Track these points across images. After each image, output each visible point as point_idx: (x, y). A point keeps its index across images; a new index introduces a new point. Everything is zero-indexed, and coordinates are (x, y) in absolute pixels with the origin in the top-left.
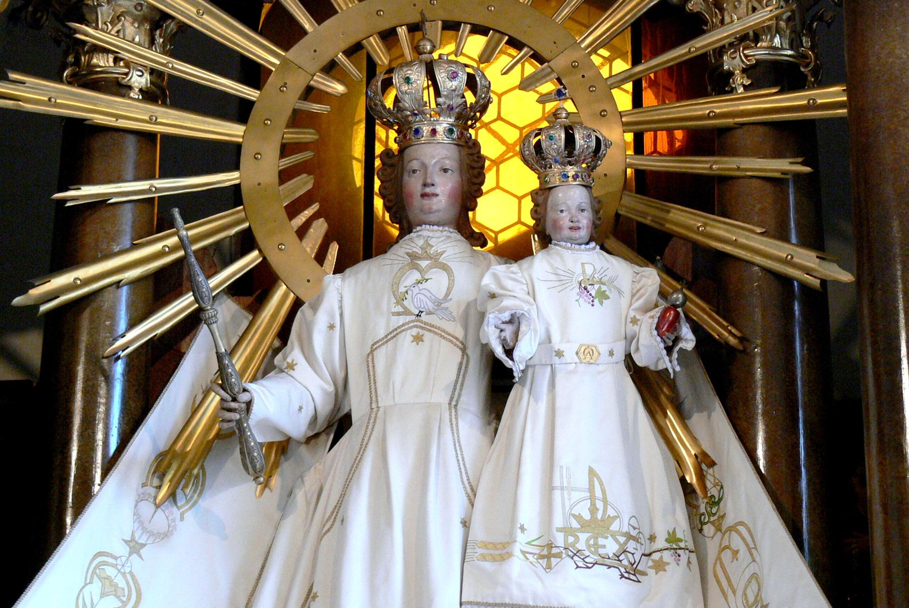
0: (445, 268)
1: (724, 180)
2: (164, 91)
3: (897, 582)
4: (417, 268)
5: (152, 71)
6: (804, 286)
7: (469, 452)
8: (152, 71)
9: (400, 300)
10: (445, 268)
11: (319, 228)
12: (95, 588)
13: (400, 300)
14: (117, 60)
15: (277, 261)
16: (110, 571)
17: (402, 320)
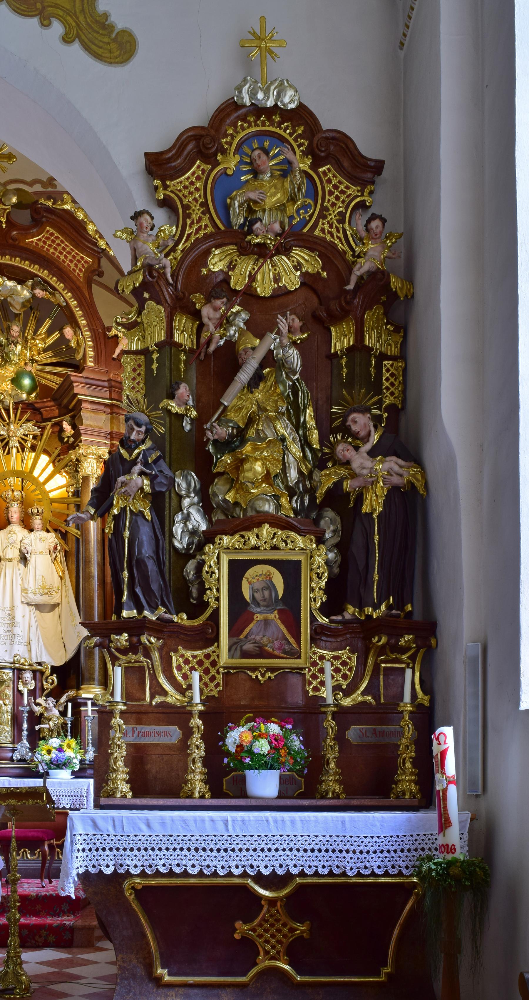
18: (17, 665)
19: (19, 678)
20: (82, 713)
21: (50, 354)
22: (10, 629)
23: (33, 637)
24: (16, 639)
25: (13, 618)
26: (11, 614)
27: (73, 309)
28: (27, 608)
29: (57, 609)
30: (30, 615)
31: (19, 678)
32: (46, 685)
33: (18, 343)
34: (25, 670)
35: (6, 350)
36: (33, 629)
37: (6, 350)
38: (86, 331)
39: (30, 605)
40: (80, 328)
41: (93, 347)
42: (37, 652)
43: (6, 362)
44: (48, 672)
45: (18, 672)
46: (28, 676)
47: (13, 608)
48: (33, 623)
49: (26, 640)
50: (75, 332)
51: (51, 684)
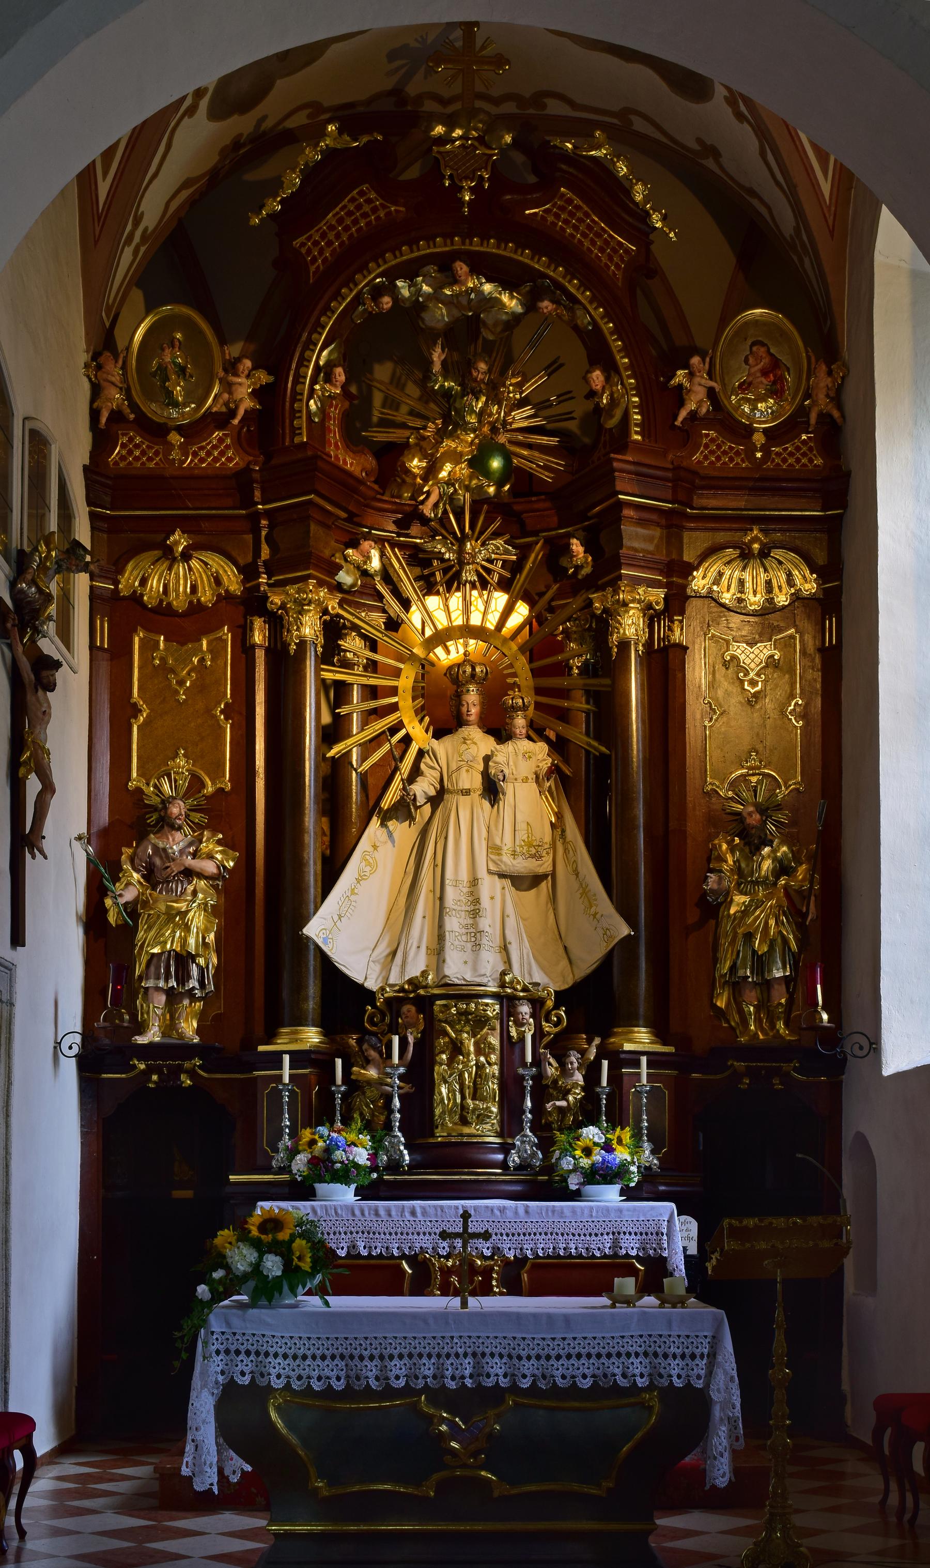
0: (475, 744)
1: (568, 710)
2: (372, 666)
3: (592, 776)
4: (465, 743)
5: (367, 659)
6: (594, 755)
7: (487, 814)
8: (367, 659)
9: (460, 756)
10: (475, 744)
11: (427, 719)
12: (364, 863)
13: (460, 756)
14: (354, 654)
15: (411, 731)
16: (368, 857)
17: (462, 763)
18: (509, 991)
19: (510, 1014)
20: (625, 1079)
21: (528, 411)
22: (470, 921)
23: (511, 936)
24: (484, 941)
25: (477, 901)
26: (472, 893)
27: (608, 335)
28: (498, 883)
29: (544, 884)
30: (503, 895)
31: (509, 1015)
32: (547, 1027)
33: (481, 391)
34: (520, 998)
35: (457, 405)
36: (511, 922)
37: (457, 405)
38: (629, 377)
39: (502, 876)
40: (618, 372)
41: (640, 406)
42: (522, 965)
43: (456, 426)
44: (550, 1004)
45: (508, 1002)
46: (525, 1009)
47: (474, 882)
48: (510, 910)
49: (498, 941)
50: (608, 379)
51: (556, 1025)
